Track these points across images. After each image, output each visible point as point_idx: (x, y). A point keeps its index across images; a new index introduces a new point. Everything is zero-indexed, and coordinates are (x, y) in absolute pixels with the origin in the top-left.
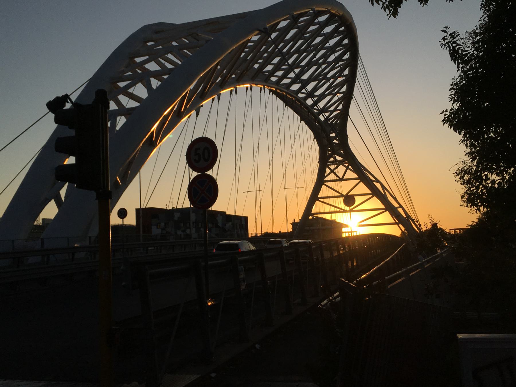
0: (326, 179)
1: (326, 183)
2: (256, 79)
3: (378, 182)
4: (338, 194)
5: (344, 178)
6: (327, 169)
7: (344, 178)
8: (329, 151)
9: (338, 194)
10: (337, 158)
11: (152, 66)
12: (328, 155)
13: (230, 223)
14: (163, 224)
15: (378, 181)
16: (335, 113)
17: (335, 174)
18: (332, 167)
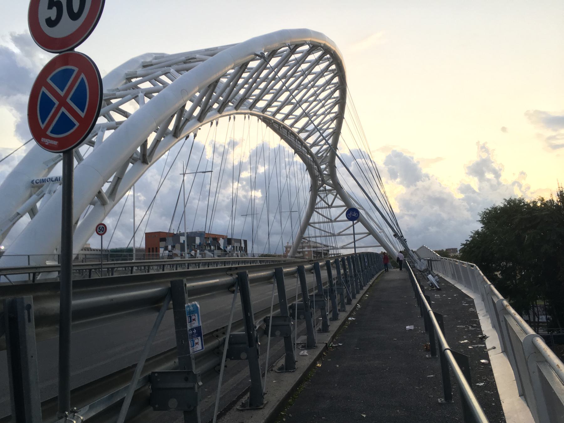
1: (318, 210)
2: (253, 109)
4: (328, 220)
5: (333, 205)
6: (318, 197)
11: (146, 85)
13: (230, 246)
14: (170, 247)
16: (325, 147)
17: (325, 202)
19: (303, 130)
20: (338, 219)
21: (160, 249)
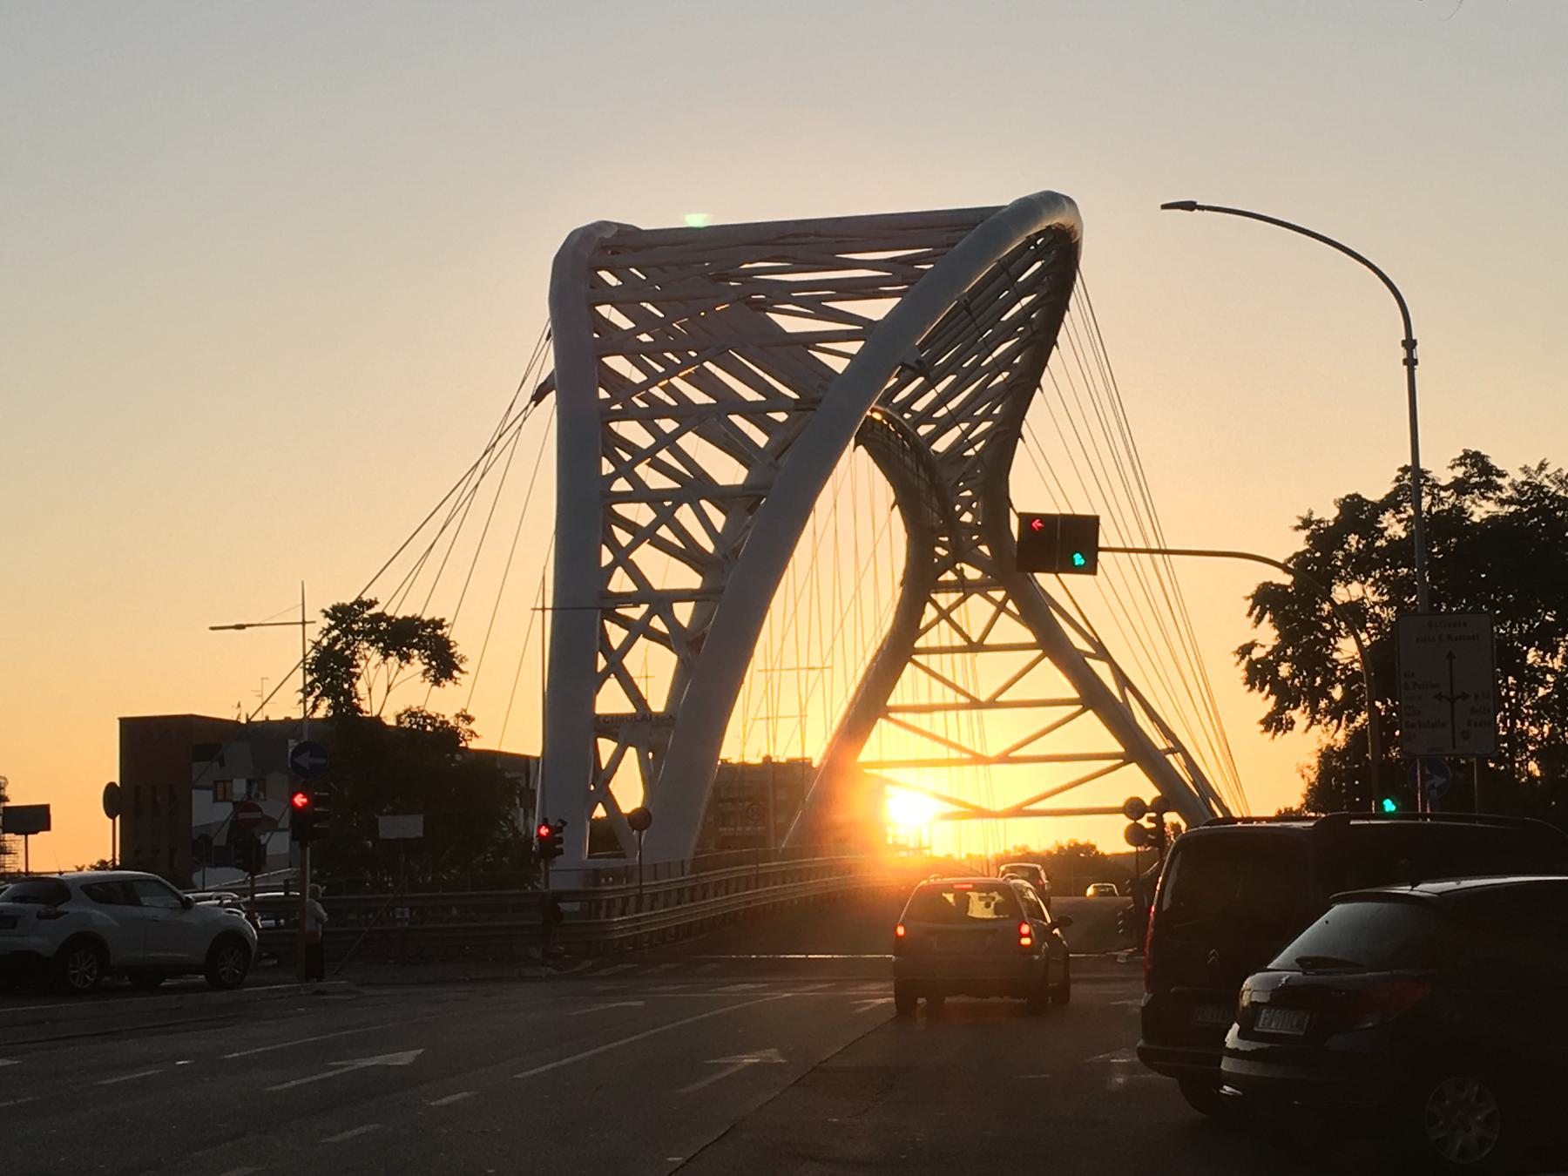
0: (919, 644)
3: (1101, 659)
4: (962, 700)
5: (985, 643)
6: (929, 606)
7: (985, 643)
8: (943, 545)
9: (962, 700)
10: (966, 574)
12: (936, 560)
14: (239, 787)
15: (1102, 653)
18: (944, 599)
19: (926, 416)
20: (999, 699)
21: (194, 791)
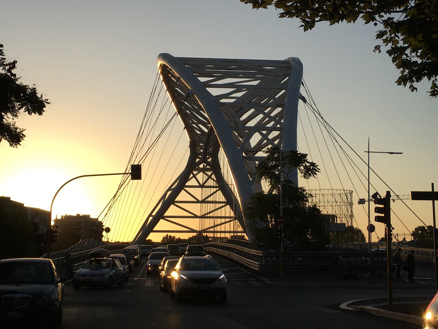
0: (187, 184)
5: (206, 184)
9: (196, 200)
13: (39, 217)
18: (195, 173)
